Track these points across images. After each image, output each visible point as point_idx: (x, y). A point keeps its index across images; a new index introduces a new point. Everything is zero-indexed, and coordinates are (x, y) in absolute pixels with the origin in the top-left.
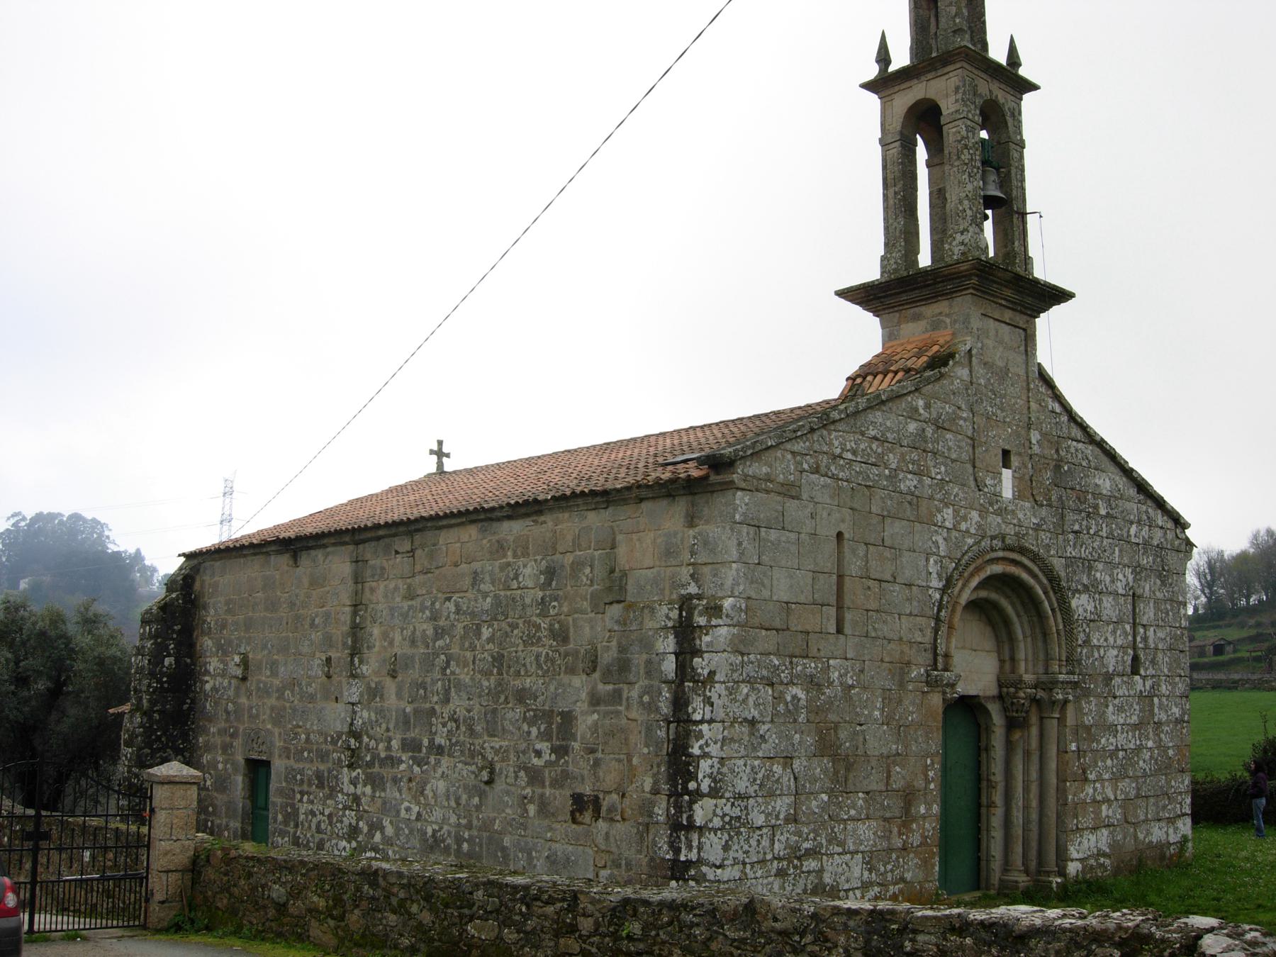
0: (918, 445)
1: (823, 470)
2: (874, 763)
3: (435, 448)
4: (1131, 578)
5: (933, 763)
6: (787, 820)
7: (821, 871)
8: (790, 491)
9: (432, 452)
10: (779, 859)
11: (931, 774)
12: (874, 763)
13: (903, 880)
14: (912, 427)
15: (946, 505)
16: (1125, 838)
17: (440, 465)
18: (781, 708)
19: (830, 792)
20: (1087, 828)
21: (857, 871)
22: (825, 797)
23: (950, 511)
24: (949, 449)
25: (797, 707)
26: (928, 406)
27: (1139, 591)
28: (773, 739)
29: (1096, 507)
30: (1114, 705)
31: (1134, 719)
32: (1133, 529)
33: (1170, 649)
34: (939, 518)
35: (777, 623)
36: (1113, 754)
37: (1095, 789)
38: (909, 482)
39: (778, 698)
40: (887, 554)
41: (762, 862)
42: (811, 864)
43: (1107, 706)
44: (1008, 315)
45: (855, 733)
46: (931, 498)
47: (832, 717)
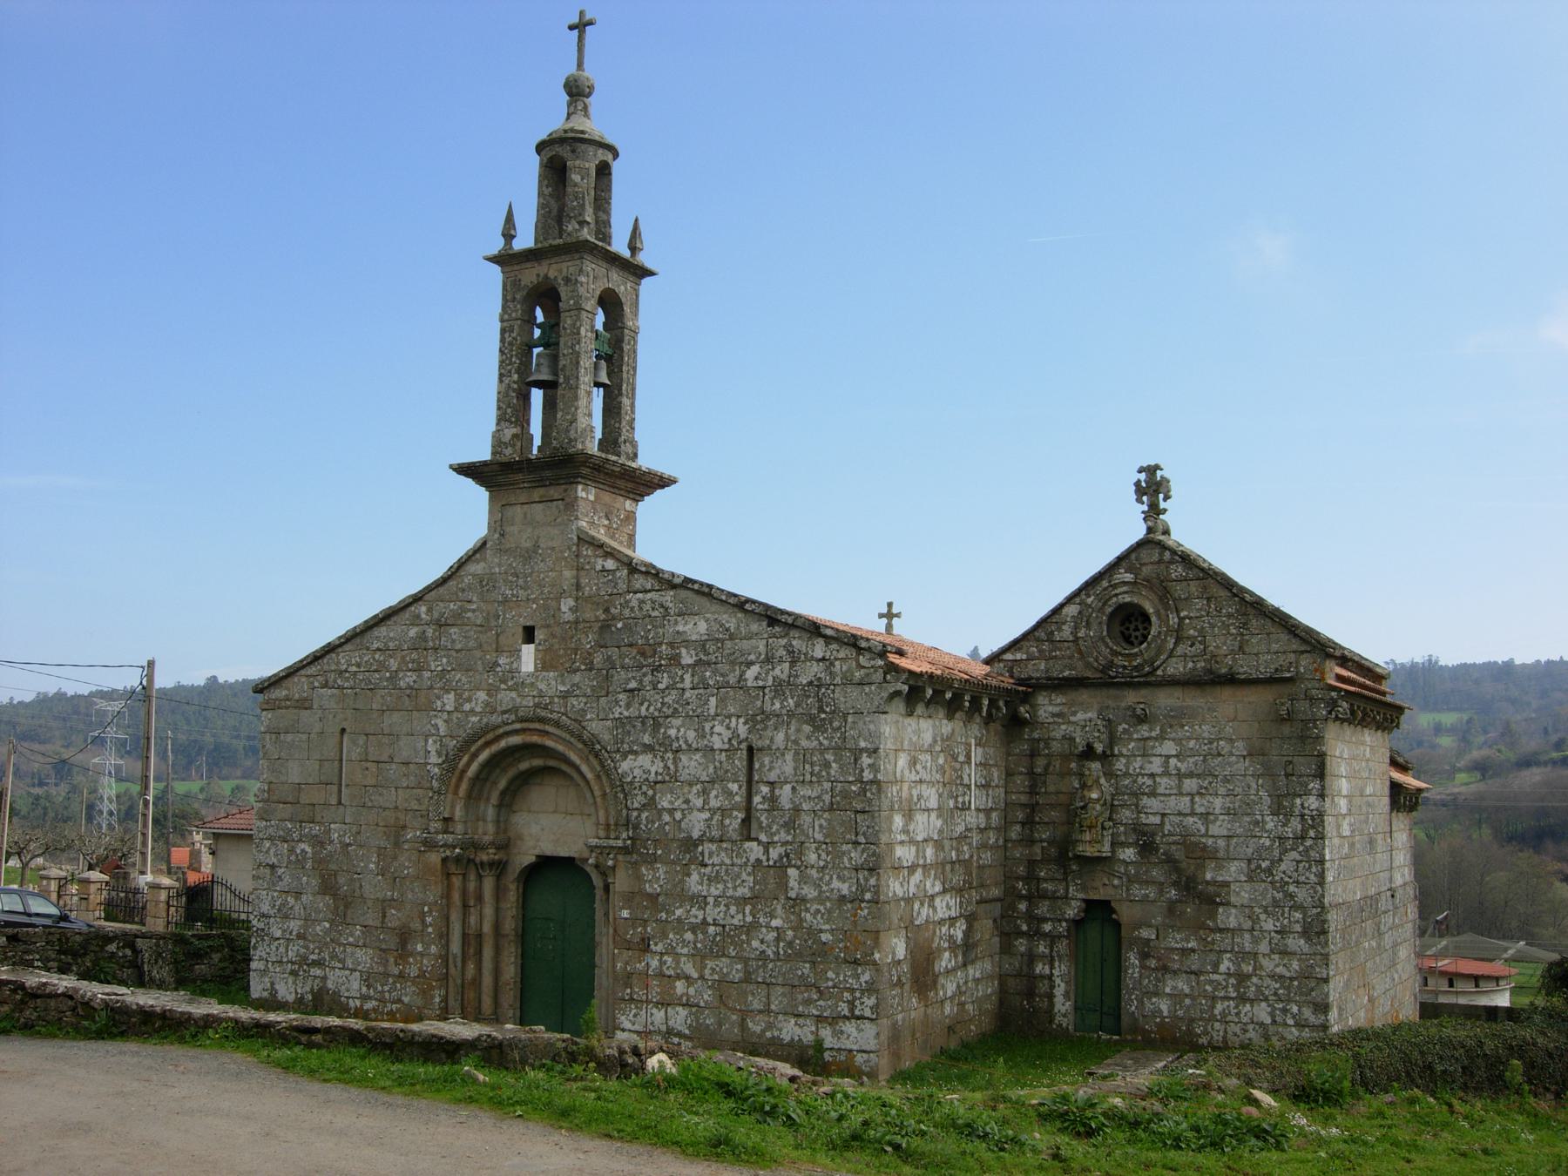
0: (419, 645)
1: (331, 683)
2: (370, 904)
3: (894, 611)
4: (743, 730)
5: (430, 911)
6: (299, 936)
7: (324, 978)
8: (304, 704)
9: (881, 616)
10: (293, 963)
11: (429, 920)
12: (370, 904)
13: (399, 1001)
14: (413, 632)
15: (448, 692)
16: (720, 1025)
17: (889, 627)
18: (293, 858)
19: (332, 922)
21: (356, 985)
22: (327, 925)
23: (452, 696)
24: (453, 641)
25: (305, 859)
26: (430, 610)
27: (757, 743)
28: (287, 879)
30: (702, 875)
31: (743, 891)
32: (751, 673)
33: (831, 809)
34: (439, 703)
35: (290, 799)
37: (662, 963)
38: (410, 678)
39: (292, 851)
40: (385, 740)
42: (317, 972)
43: (689, 875)
44: (537, 494)
45: (352, 880)
46: (431, 688)
47: (333, 867)
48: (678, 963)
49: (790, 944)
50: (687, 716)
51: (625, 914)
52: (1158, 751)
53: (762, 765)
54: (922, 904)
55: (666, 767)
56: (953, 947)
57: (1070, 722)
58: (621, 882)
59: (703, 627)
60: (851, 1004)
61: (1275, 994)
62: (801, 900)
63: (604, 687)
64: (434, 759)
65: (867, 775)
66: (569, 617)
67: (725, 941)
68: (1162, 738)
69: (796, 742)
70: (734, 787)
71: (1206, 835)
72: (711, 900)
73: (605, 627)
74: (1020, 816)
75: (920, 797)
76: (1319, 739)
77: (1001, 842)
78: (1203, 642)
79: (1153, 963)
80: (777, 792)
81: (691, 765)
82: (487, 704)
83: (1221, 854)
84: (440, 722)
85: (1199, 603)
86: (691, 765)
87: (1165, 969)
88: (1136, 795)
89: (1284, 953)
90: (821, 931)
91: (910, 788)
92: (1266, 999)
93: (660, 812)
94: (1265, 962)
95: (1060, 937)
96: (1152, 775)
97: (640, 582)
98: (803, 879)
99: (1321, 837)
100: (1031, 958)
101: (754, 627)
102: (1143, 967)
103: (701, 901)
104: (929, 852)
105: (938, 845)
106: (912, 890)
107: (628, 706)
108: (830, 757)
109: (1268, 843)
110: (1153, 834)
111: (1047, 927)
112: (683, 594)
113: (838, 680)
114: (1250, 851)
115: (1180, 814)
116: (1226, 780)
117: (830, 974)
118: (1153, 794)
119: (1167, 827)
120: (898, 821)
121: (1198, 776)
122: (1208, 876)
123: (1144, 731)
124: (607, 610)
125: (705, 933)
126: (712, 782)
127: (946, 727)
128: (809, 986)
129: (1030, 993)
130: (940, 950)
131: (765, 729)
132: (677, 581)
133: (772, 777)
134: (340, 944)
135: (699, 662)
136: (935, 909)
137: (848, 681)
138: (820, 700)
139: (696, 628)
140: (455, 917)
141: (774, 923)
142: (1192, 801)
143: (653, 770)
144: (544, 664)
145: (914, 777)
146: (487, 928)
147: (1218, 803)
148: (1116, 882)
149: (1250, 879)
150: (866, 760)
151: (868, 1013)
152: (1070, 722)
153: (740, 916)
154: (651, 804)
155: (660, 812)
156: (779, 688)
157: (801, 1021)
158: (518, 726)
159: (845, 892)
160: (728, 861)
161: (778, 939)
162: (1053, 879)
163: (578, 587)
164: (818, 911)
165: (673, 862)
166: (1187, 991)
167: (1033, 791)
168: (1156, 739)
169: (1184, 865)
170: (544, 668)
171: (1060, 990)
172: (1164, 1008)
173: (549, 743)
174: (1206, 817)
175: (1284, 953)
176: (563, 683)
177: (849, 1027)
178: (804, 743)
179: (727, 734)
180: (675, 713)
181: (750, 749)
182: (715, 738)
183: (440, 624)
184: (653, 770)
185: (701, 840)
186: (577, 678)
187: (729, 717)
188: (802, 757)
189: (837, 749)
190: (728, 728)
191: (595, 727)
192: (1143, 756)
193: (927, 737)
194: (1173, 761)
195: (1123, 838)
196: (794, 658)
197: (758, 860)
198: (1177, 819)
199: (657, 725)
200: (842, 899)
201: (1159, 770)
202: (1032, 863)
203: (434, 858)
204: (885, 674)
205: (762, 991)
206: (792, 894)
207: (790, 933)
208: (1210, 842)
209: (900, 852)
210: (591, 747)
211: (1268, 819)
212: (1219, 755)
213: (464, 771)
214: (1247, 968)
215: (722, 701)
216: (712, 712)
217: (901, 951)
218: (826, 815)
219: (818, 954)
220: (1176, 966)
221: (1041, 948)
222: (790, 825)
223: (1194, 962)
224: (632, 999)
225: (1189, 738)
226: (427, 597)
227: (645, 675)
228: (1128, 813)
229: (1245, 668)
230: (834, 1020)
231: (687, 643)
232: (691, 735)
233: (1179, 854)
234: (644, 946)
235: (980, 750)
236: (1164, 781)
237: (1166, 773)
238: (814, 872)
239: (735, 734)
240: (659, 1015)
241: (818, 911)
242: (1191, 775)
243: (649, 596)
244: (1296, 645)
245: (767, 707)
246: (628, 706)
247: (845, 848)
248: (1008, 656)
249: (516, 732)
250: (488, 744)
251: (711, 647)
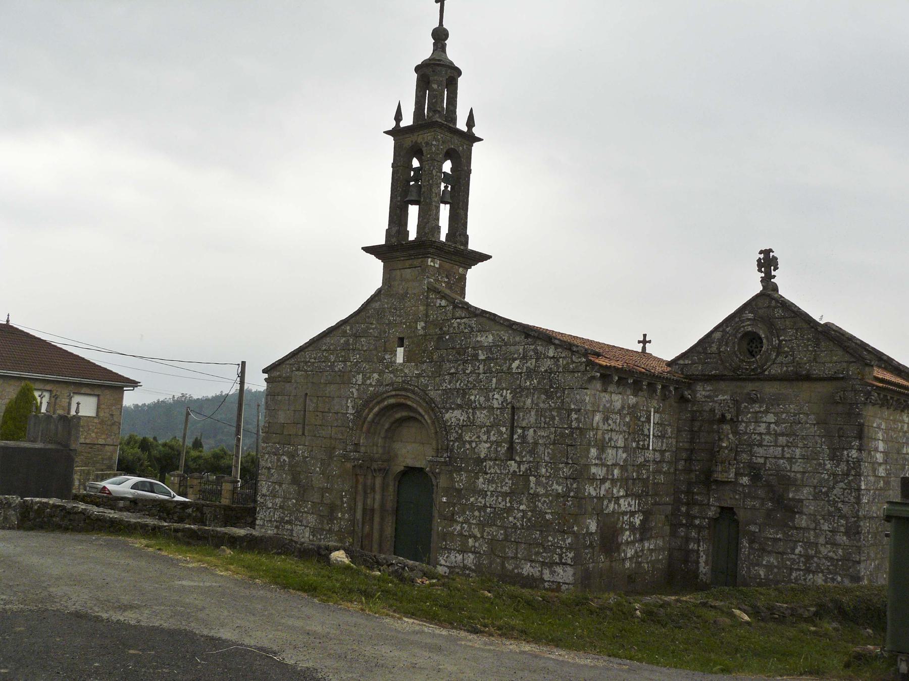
0: (346, 347)
4: (509, 397)
5: (346, 495)
6: (281, 507)
7: (292, 530)
8: (288, 380)
9: (639, 342)
11: (345, 499)
16: (491, 564)
17: (644, 348)
20: (454, 550)
21: (307, 535)
23: (361, 376)
26: (351, 329)
28: (276, 476)
29: (476, 355)
30: (485, 479)
32: (515, 364)
33: (554, 444)
36: (480, 509)
37: (462, 528)
38: (340, 366)
39: (278, 460)
40: (327, 400)
41: (270, 521)
46: (351, 371)
47: (298, 469)
48: (470, 528)
49: (529, 520)
50: (481, 389)
51: (444, 499)
52: (764, 419)
53: (519, 417)
54: (610, 501)
55: (468, 417)
56: (632, 528)
58: (443, 482)
59: (491, 338)
60: (560, 556)
61: (828, 569)
62: (536, 495)
63: (438, 373)
64: (351, 411)
65: (574, 424)
66: (421, 332)
67: (497, 516)
68: (767, 412)
69: (537, 405)
70: (504, 429)
71: (790, 471)
72: (489, 493)
73: (440, 338)
74: (684, 455)
75: (610, 439)
76: (859, 415)
77: (672, 470)
78: (792, 355)
79: (756, 546)
80: (526, 433)
81: (482, 416)
82: (378, 380)
83: (799, 482)
84: (354, 390)
85: (791, 332)
86: (482, 416)
87: (763, 550)
88: (751, 445)
89: (835, 544)
90: (546, 513)
91: (603, 434)
92: (822, 572)
93: (464, 442)
94: (822, 549)
96: (760, 434)
97: (459, 313)
98: (538, 483)
99: (859, 475)
100: (687, 539)
101: (517, 339)
102: (751, 548)
103: (483, 494)
104: (616, 472)
105: (623, 468)
106: (602, 492)
107: (450, 383)
108: (555, 413)
109: (826, 477)
110: (759, 469)
111: (697, 522)
112: (482, 320)
113: (561, 370)
114: (815, 481)
115: (775, 458)
116: (804, 438)
117: (550, 538)
118: (760, 445)
119: (768, 465)
120: (593, 452)
121: (787, 435)
122: (791, 496)
123: (756, 407)
124: (441, 329)
125: (485, 512)
126: (492, 426)
127: (632, 400)
128: (538, 545)
129: (686, 561)
130: (623, 530)
131: (521, 397)
132: (478, 312)
133: (524, 424)
134: (301, 512)
135: (488, 358)
136: (619, 505)
137: (566, 370)
138: (551, 381)
139: (487, 339)
140: (360, 499)
141: (522, 507)
142: (783, 451)
143: (462, 419)
144: (408, 358)
145: (606, 427)
146: (377, 506)
149: (815, 499)
150: (574, 416)
151: (569, 561)
153: (504, 503)
154: (460, 438)
155: (464, 442)
156: (530, 373)
157: (533, 564)
158: (394, 393)
159: (560, 491)
160: (498, 472)
161: (523, 517)
163: (427, 315)
164: (545, 501)
165: (470, 471)
167: (692, 441)
170: (408, 361)
171: (702, 560)
172: (762, 573)
173: (409, 403)
174: (791, 460)
175: (835, 544)
176: (417, 370)
177: (559, 570)
178: (542, 405)
179: (501, 399)
180: (474, 387)
181: (513, 408)
182: (495, 402)
183: (356, 336)
184: (462, 419)
185: (485, 460)
186: (424, 367)
187: (502, 389)
188: (540, 413)
189: (559, 409)
190: (502, 396)
191: (432, 394)
192: (756, 422)
193: (618, 405)
194: (772, 426)
195: (742, 471)
196: (538, 357)
197: (515, 471)
198: (773, 461)
199: (464, 394)
200: (558, 495)
201: (764, 431)
202: (690, 484)
203: (349, 465)
204: (586, 366)
205: (513, 546)
206: (532, 491)
207: (530, 513)
209: (594, 470)
210: (430, 404)
211: (827, 462)
212: (800, 423)
213: (366, 418)
214: (811, 552)
215: (499, 382)
216: (494, 386)
217: (593, 527)
218: (551, 447)
219: (544, 527)
221: (693, 534)
222: (532, 452)
223: (781, 547)
224: (446, 548)
225: (783, 413)
226: (351, 321)
227: (459, 365)
229: (816, 371)
230: (551, 565)
231: (482, 347)
232: (482, 399)
234: (451, 519)
235: (657, 415)
236: (767, 438)
237: (769, 433)
238: (544, 479)
239: (505, 400)
240: (460, 557)
241: (545, 501)
242: (782, 434)
243: (463, 321)
244: (847, 358)
245: (523, 385)
246: (450, 383)
247: (561, 466)
248: (681, 362)
249: (393, 396)
250: (378, 403)
251: (494, 350)
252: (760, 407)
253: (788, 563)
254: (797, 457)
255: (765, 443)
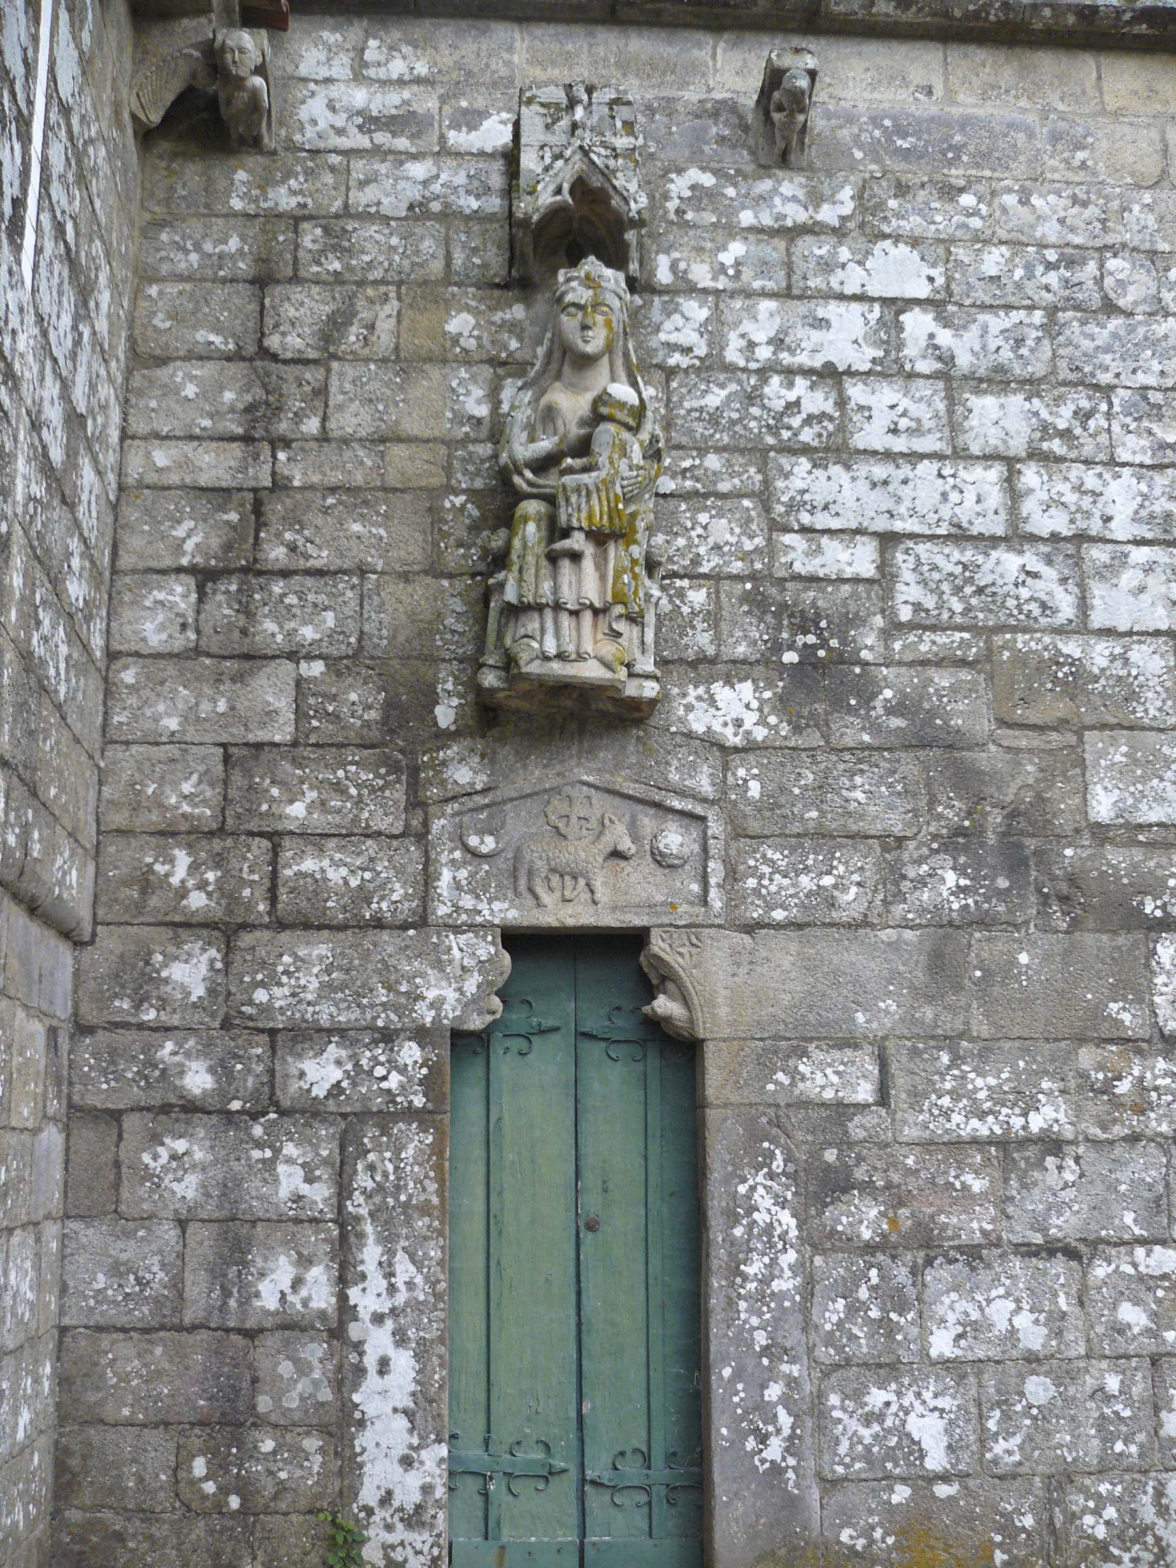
52: (852, 279)
57: (445, 152)
68: (866, 228)
71: (1081, 627)
74: (193, 538)
79: (864, 1218)
87: (928, 1244)
95: (387, 1116)
96: (830, 375)
100: (235, 1232)
102: (818, 1240)
110: (850, 621)
111: (321, 1072)
115: (960, 536)
116: (1147, 406)
118: (836, 450)
119: (909, 593)
121: (1032, 386)
122: (1103, 805)
123: (787, 197)
129: (229, 1421)
147: (1121, 497)
148: (674, 839)
152: (445, 152)
162: (351, 835)
166: (1033, 1337)
167: (258, 430)
168: (839, 233)
169: (989, 758)
171: (387, 1394)
172: (930, 1433)
174: (1069, 547)
192: (786, 294)
194: (917, 323)
195: (702, 639)
198: (949, 559)
202: (240, 757)
208: (1100, 654)
212: (1110, 308)
220: (976, 1224)
223: (1060, 1198)
225: (982, 240)
228: (723, 530)
233: (966, 710)
236: (882, 398)
237: (891, 369)
242: (998, 380)
252: (816, 199)
253: (1132, 1315)
254: (1121, 529)
255: (871, 436)
